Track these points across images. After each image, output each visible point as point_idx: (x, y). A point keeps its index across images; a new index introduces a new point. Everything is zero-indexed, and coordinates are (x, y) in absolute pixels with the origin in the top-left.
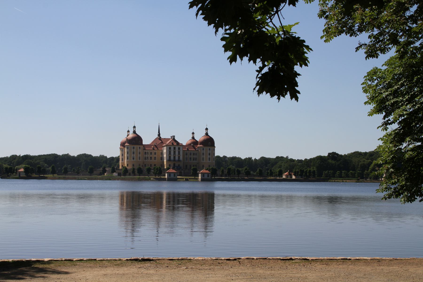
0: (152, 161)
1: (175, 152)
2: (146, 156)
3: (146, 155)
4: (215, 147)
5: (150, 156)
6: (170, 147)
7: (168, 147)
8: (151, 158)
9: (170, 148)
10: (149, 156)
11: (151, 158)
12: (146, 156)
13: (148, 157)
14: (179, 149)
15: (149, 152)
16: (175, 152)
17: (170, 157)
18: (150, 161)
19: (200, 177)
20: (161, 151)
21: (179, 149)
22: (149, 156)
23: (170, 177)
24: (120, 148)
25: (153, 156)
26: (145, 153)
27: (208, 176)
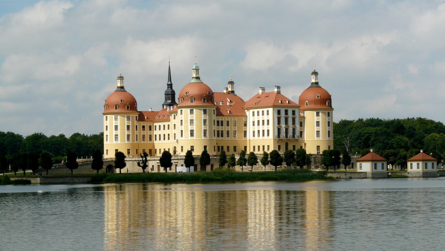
0: (229, 138)
1: (286, 119)
2: (220, 128)
3: (220, 127)
4: (333, 109)
5: (226, 130)
6: (279, 109)
7: (276, 109)
8: (228, 132)
9: (279, 112)
10: (225, 129)
11: (228, 132)
12: (219, 128)
13: (222, 131)
14: (294, 113)
15: (223, 120)
16: (286, 119)
17: (279, 130)
18: (227, 138)
19: (420, 170)
20: (244, 120)
21: (294, 113)
22: (225, 128)
23: (375, 170)
24: (102, 113)
25: (231, 128)
26: (218, 122)
27: (418, 168)
